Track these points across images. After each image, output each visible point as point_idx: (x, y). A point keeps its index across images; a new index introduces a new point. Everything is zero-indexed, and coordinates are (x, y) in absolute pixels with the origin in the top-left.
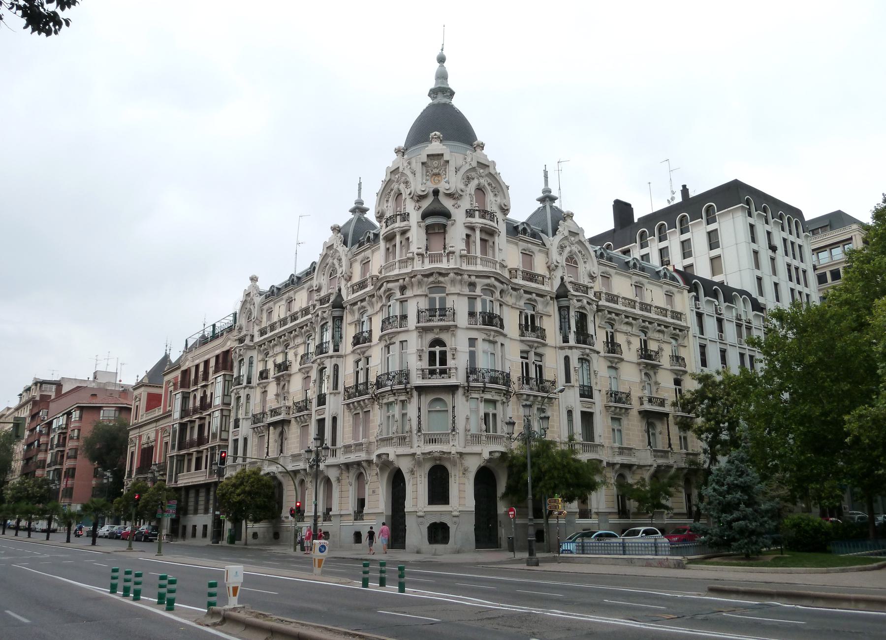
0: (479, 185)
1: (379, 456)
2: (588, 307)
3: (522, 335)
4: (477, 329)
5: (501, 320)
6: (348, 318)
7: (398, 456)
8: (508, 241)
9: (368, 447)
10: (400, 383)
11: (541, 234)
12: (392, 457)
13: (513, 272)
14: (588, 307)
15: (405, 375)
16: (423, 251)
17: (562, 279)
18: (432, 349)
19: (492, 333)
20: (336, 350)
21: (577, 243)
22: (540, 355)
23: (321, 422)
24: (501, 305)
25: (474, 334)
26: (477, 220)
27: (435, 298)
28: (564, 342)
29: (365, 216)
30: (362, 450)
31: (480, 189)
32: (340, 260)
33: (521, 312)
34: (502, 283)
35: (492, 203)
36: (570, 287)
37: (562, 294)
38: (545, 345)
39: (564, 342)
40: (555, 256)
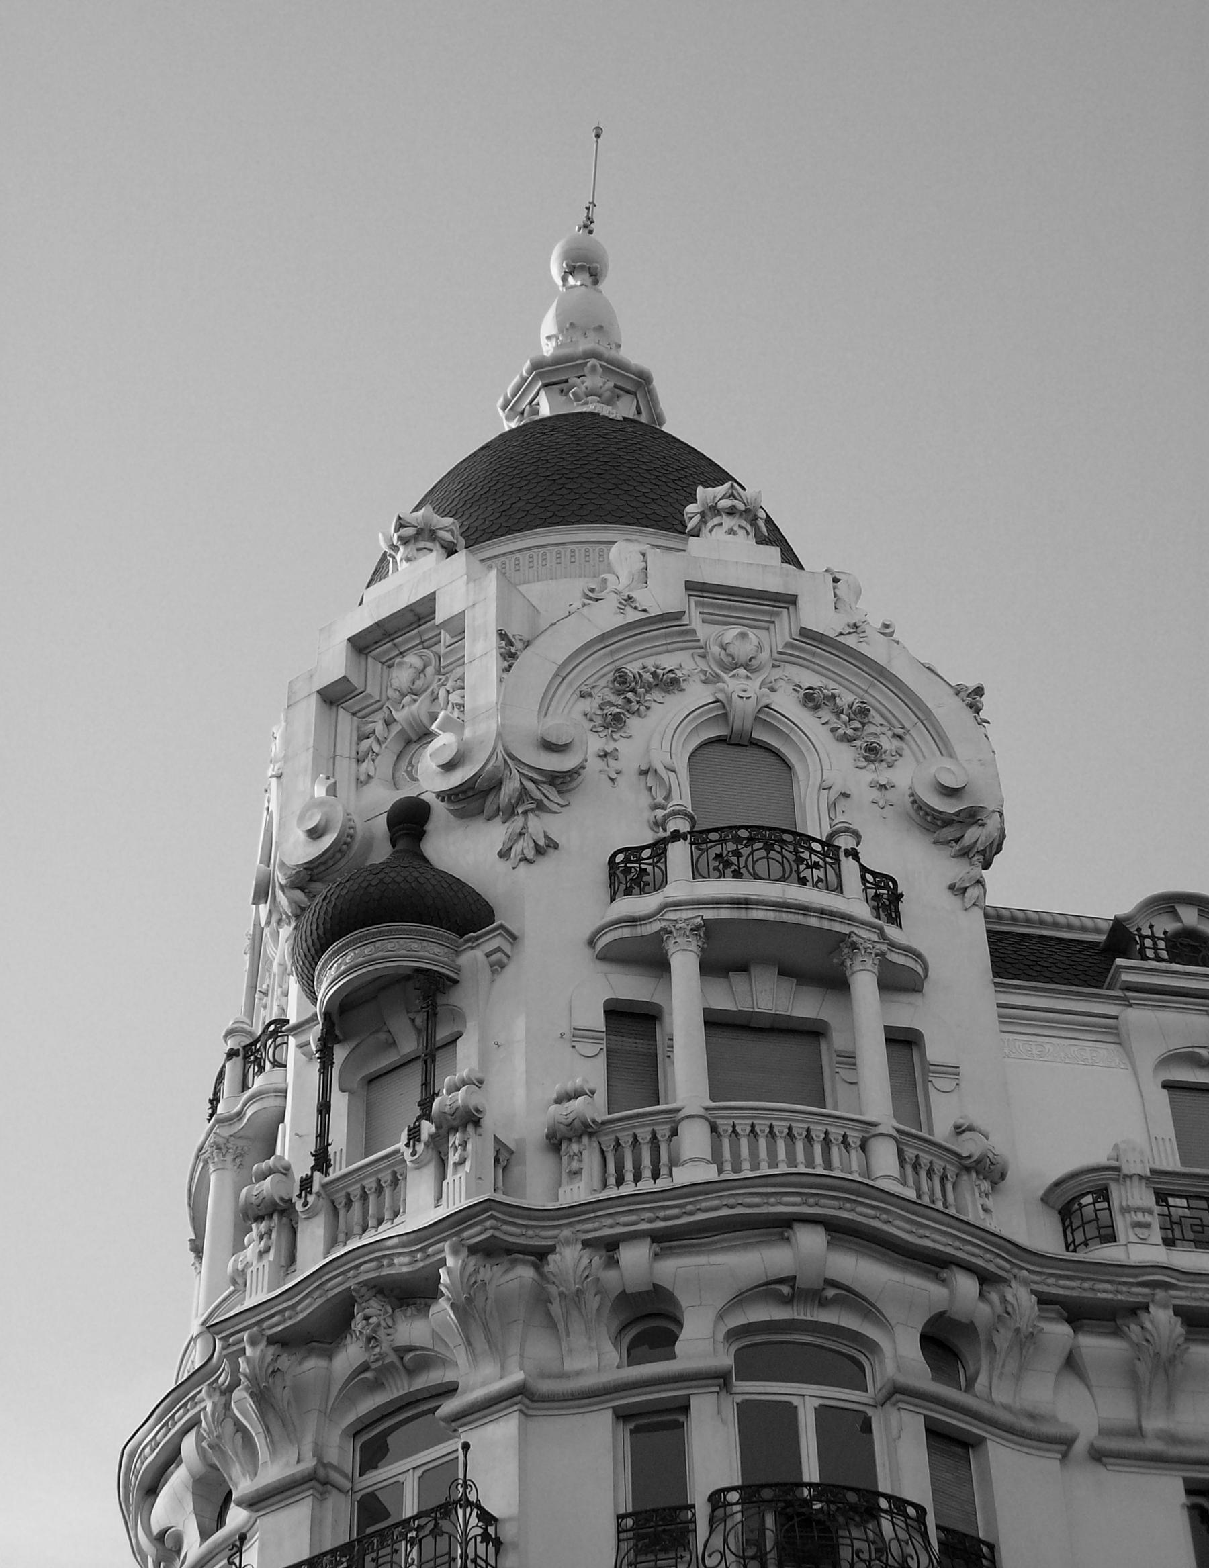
0: (722, 710)
8: (1008, 1016)
13: (1080, 1203)
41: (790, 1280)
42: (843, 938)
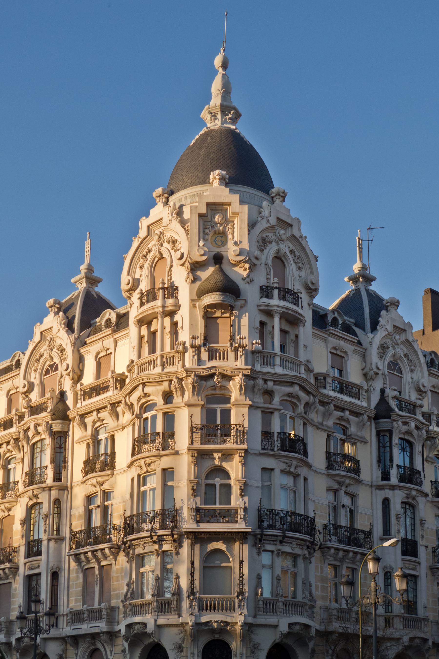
1: (129, 626)
2: (415, 432)
3: (330, 467)
4: (274, 456)
5: (305, 445)
6: (77, 433)
7: (159, 627)
9: (108, 614)
10: (163, 527)
11: (354, 328)
12: (150, 628)
13: (321, 380)
14: (415, 432)
15: (169, 516)
16: (199, 342)
17: (383, 391)
18: (210, 481)
19: (295, 463)
20: (58, 478)
21: (403, 343)
22: (353, 497)
23: (32, 580)
24: (304, 424)
25: (270, 463)
26: (275, 302)
27: (215, 411)
28: (383, 479)
29: (96, 289)
30: (99, 618)
31: (279, 259)
32: (63, 351)
33: (328, 436)
34: (308, 393)
35: (294, 281)
36: (393, 404)
37: (383, 412)
38: (359, 482)
39: (383, 479)
40: (374, 359)
41: (291, 394)
42: (299, 319)
